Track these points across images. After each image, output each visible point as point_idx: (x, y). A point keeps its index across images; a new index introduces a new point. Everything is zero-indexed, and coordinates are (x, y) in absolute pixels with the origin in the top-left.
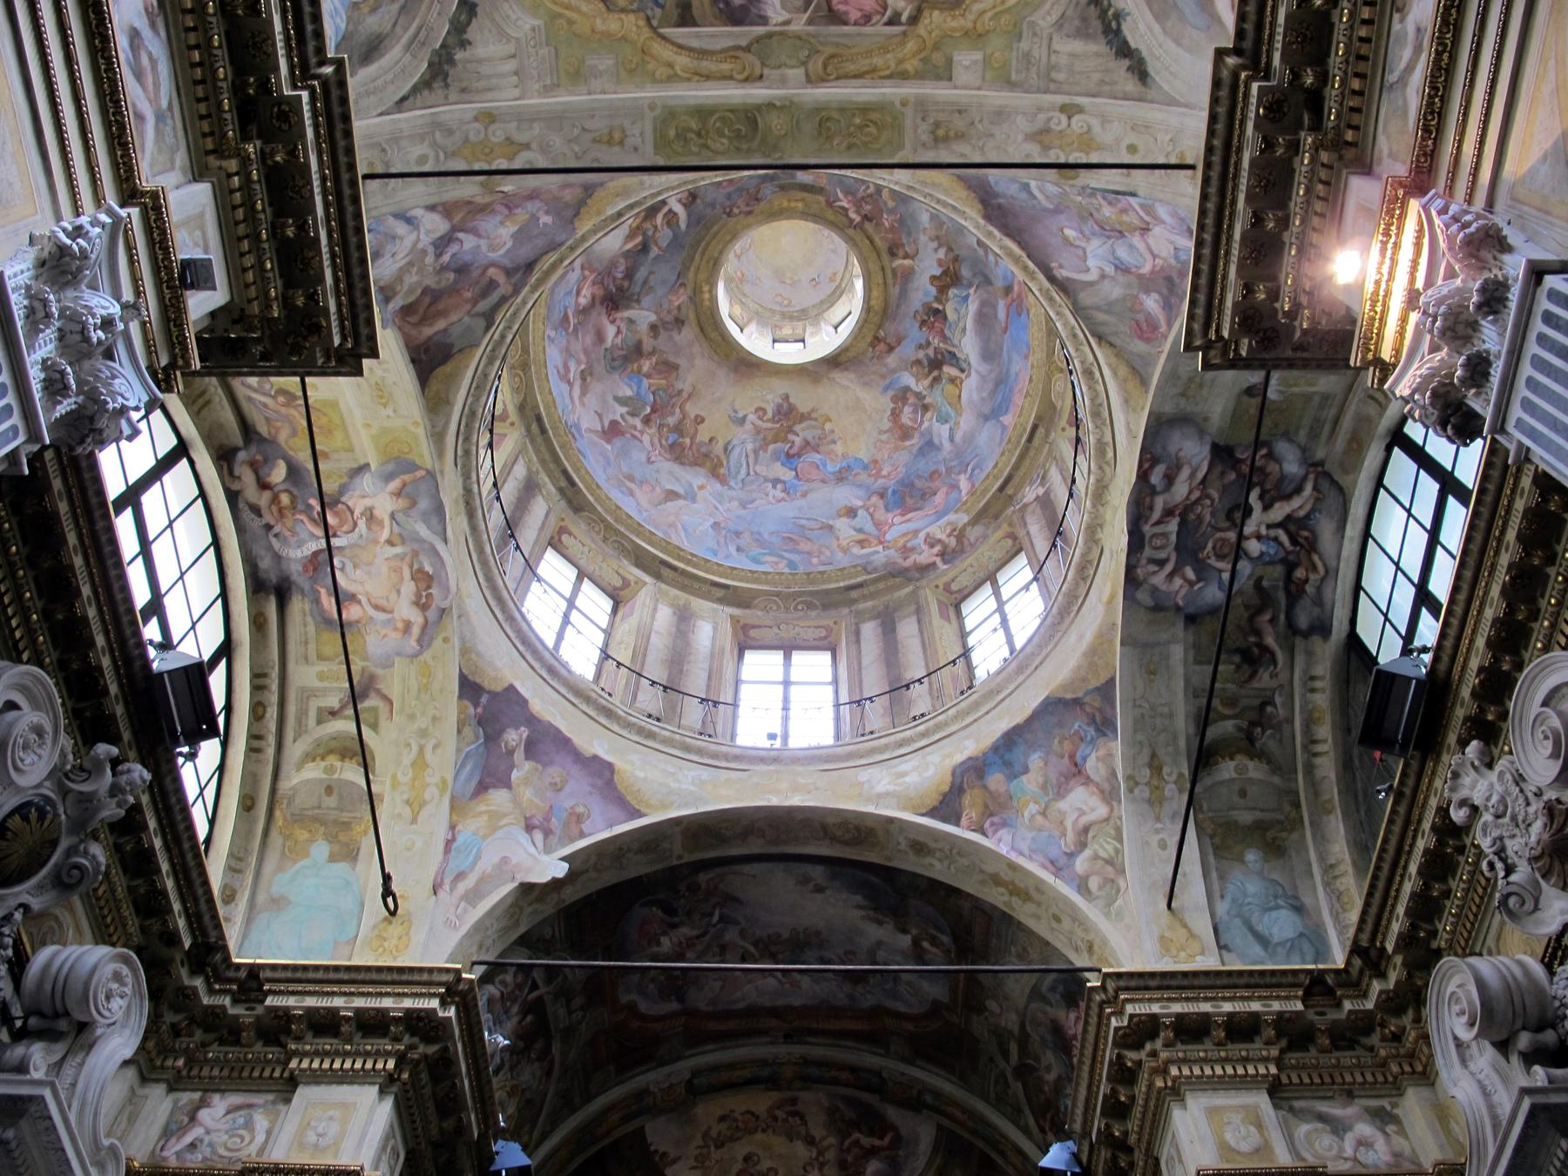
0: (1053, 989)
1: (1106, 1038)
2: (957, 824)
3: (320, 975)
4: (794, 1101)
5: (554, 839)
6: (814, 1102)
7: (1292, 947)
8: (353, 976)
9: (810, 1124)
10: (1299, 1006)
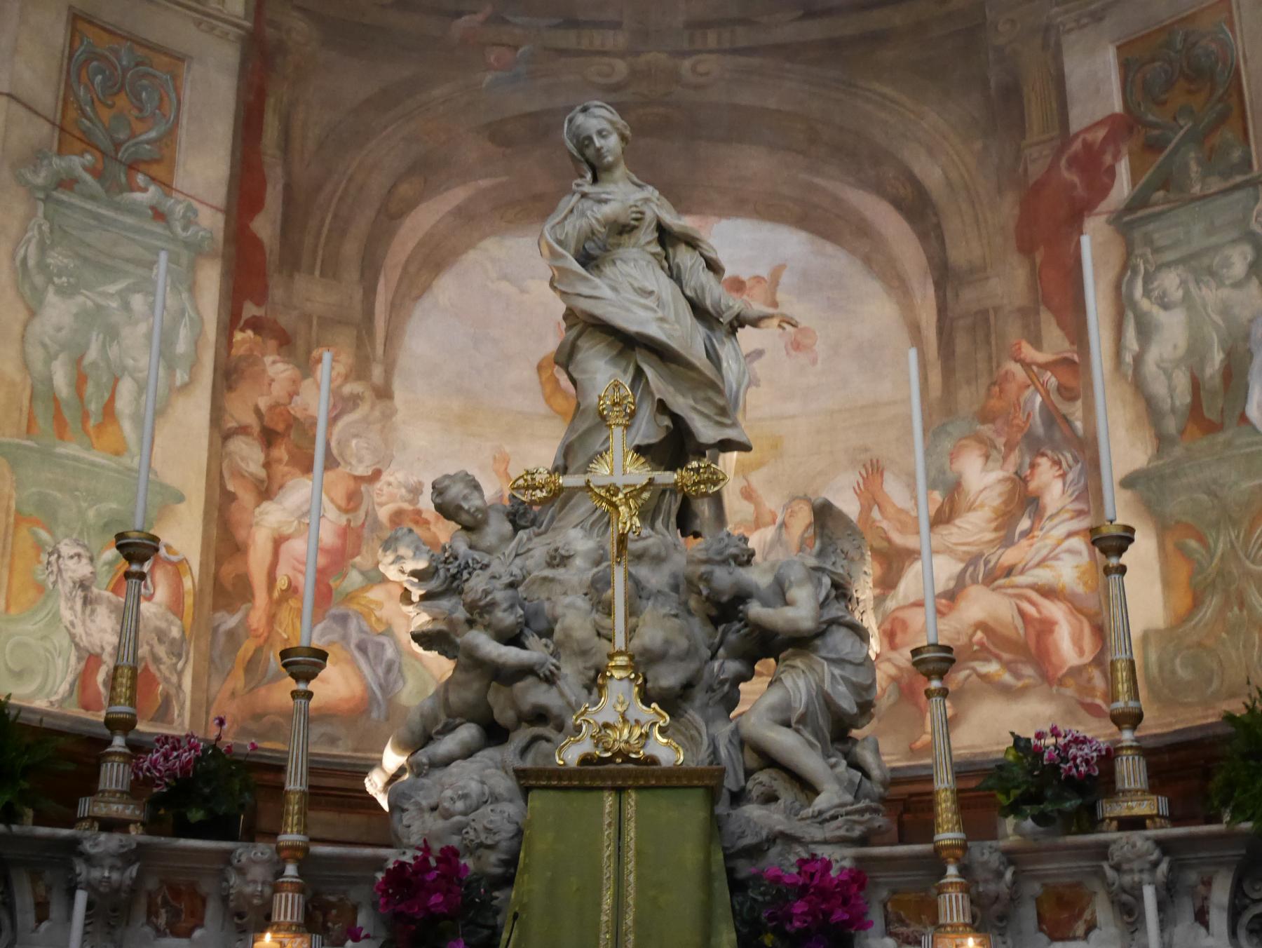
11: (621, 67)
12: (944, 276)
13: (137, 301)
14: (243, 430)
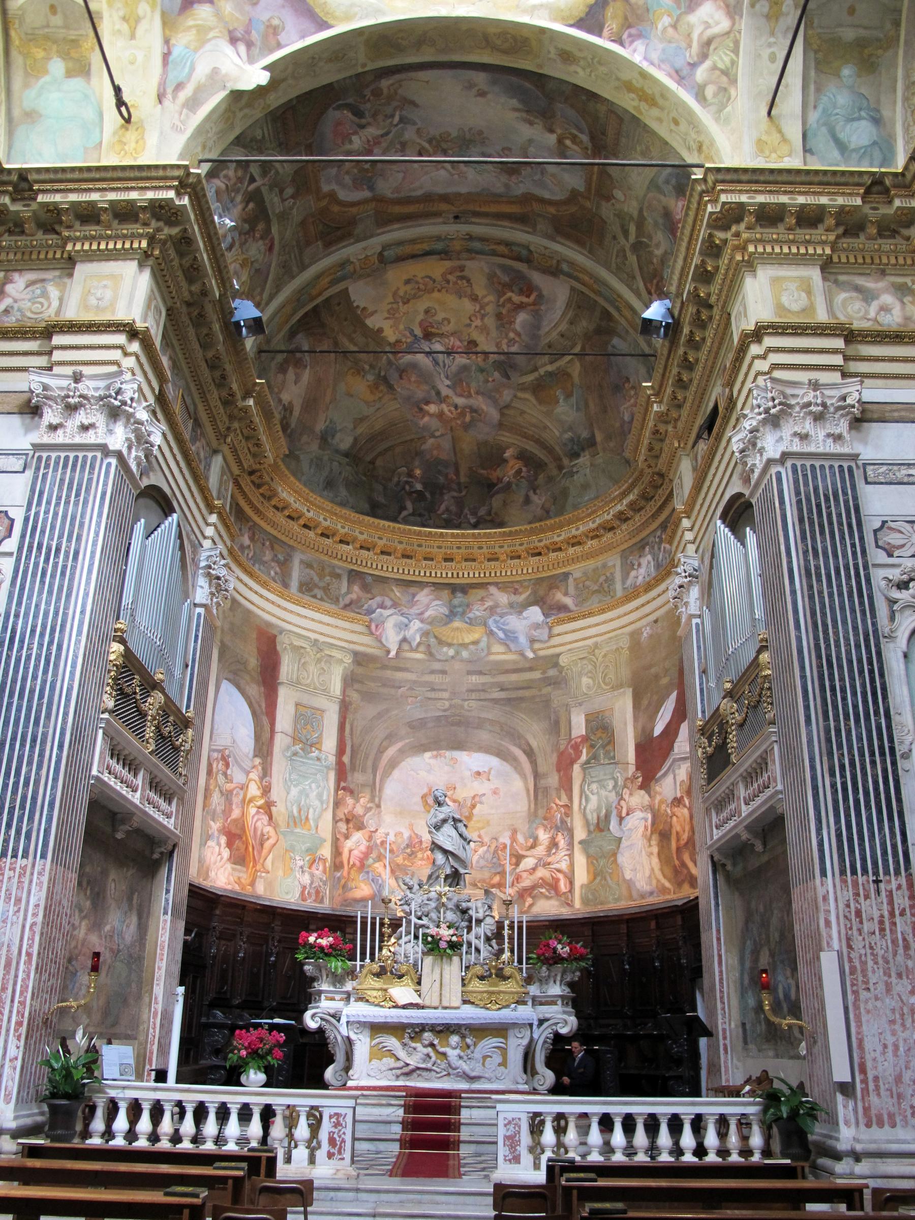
0: (667, 182)
1: (702, 221)
2: (600, 36)
3: (76, 175)
4: (462, 269)
5: (256, 51)
7: (864, 153)
8: (103, 175)
9: (474, 286)
10: (858, 201)
11: (447, 704)
12: (536, 775)
13: (313, 785)
14: (341, 820)
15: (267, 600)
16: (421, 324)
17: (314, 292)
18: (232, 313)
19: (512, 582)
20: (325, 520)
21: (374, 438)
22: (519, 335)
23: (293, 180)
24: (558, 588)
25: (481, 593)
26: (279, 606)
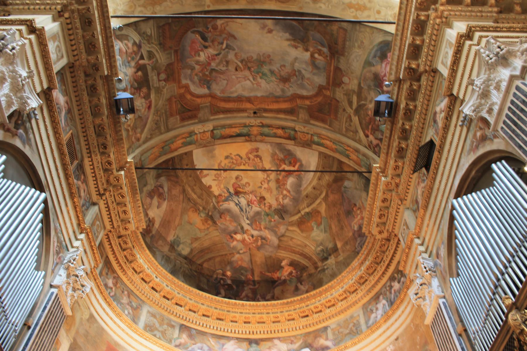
0: (375, 56)
4: (257, 150)
6: (266, 150)
9: (264, 162)
15: (119, 326)
16: (233, 185)
17: (173, 146)
18: (115, 96)
19: (289, 337)
20: (167, 286)
21: (203, 251)
22: (289, 191)
23: (166, 70)
24: (321, 336)
25: (269, 344)
26: (127, 334)
